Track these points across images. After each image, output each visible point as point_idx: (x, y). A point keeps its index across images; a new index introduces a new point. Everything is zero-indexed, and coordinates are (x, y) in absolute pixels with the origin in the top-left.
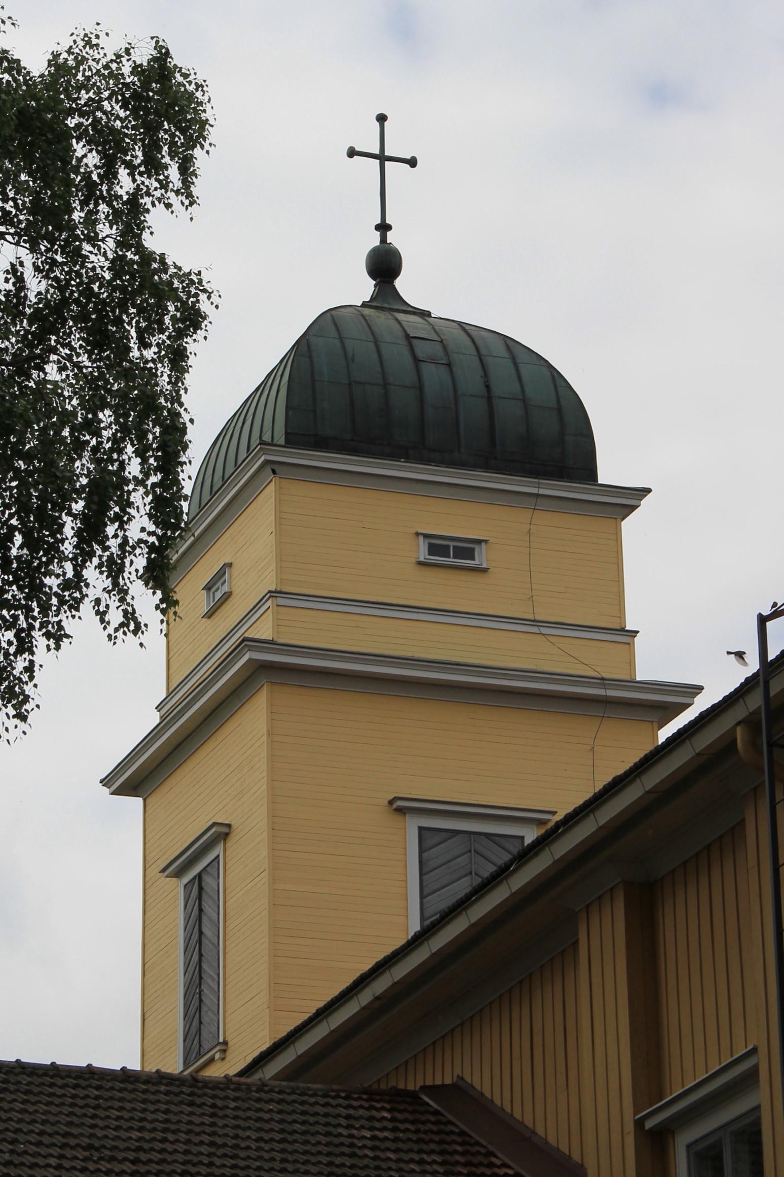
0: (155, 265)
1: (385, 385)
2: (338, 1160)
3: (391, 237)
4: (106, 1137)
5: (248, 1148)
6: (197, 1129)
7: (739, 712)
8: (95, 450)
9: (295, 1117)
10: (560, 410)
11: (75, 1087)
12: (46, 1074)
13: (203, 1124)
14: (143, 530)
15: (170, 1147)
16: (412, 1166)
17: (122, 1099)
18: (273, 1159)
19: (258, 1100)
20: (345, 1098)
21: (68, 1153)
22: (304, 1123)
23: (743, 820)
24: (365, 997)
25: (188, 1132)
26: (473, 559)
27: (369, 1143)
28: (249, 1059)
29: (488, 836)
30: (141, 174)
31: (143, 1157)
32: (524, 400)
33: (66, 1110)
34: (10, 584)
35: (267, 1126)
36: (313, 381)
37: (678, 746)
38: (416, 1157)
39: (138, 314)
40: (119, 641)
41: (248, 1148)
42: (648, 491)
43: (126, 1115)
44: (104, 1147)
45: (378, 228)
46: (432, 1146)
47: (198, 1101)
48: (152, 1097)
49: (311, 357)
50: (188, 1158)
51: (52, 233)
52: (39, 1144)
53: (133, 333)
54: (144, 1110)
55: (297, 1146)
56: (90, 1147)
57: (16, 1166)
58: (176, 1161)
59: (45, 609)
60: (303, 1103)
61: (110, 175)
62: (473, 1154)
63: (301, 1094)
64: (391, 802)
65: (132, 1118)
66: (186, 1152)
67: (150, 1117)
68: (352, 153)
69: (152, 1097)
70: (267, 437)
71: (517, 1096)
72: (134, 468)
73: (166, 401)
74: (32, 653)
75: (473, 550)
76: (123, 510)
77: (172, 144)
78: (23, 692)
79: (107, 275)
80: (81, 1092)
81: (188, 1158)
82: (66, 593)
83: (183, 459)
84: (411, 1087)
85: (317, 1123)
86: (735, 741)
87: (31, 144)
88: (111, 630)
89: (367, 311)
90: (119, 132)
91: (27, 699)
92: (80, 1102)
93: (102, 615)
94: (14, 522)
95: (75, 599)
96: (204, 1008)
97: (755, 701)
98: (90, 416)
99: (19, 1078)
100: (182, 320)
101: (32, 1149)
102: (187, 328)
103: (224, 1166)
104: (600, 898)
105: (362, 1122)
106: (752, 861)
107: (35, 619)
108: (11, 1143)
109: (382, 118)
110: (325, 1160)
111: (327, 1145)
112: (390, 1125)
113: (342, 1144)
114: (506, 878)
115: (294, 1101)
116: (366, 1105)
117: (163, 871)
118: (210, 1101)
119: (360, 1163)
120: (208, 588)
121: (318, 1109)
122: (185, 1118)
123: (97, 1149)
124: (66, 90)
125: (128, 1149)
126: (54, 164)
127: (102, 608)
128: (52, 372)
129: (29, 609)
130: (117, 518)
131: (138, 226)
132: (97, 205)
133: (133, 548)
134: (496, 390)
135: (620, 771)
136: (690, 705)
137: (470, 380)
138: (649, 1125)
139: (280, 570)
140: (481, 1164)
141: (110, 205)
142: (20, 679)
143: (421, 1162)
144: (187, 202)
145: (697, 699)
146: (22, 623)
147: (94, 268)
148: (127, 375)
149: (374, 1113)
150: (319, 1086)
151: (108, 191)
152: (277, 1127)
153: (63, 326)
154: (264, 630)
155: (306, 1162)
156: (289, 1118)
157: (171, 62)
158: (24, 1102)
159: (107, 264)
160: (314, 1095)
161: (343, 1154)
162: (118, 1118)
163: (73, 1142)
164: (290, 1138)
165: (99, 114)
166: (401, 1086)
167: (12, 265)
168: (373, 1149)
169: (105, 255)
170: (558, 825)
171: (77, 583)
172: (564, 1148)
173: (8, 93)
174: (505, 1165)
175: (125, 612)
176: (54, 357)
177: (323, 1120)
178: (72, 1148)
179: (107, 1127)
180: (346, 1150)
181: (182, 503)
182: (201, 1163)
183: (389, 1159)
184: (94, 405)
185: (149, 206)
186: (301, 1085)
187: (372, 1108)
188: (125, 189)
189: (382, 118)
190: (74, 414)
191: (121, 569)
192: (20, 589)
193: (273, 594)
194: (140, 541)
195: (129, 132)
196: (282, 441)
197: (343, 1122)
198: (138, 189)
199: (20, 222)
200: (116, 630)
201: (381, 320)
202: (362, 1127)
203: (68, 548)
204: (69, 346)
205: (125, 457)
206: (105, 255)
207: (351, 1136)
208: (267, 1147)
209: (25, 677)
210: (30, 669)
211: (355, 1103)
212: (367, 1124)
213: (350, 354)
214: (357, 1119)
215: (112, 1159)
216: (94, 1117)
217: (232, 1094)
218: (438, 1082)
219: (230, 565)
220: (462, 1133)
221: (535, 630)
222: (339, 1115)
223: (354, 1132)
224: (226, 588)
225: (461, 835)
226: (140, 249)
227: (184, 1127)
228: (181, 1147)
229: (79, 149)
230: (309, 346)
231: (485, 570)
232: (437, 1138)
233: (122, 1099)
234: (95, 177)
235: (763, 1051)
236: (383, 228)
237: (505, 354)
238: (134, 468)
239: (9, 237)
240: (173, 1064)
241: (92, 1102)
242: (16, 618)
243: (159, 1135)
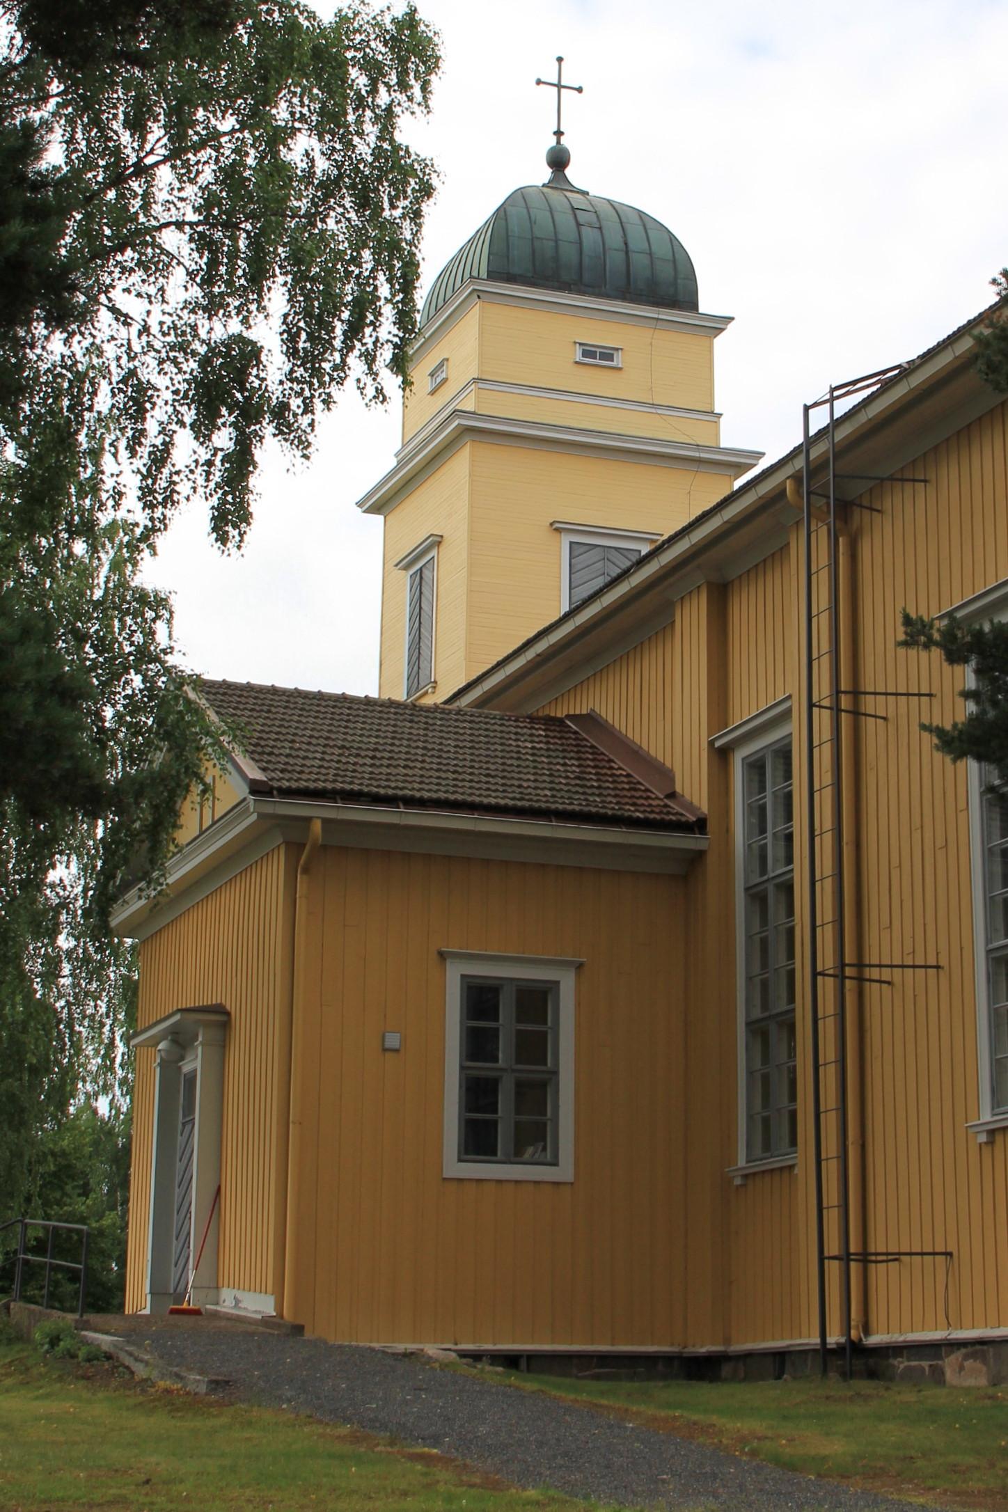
0: (402, 153)
1: (556, 241)
2: (509, 762)
3: (563, 140)
4: (354, 741)
5: (449, 751)
6: (415, 738)
7: (789, 470)
8: (358, 277)
9: (481, 732)
10: (674, 261)
11: (334, 707)
12: (314, 698)
13: (419, 735)
14: (390, 333)
15: (396, 749)
16: (558, 767)
17: (365, 716)
18: (465, 760)
19: (456, 720)
20: (515, 721)
21: (329, 750)
22: (486, 736)
23: (789, 543)
24: (530, 654)
25: (408, 740)
26: (612, 361)
27: (530, 751)
28: (451, 694)
29: (616, 549)
30: (395, 91)
31: (378, 755)
32: (650, 254)
33: (328, 722)
34: (299, 367)
35: (462, 738)
36: (508, 236)
37: (745, 493)
38: (561, 761)
39: (389, 186)
40: (372, 408)
41: (449, 751)
42: (733, 319)
43: (368, 727)
44: (352, 747)
45: (555, 133)
46: (572, 754)
47: (416, 719)
48: (386, 716)
49: (506, 220)
50: (408, 756)
51: (333, 129)
52: (309, 743)
53: (386, 199)
54: (380, 724)
55: (481, 752)
56: (343, 747)
57: (293, 757)
58: (400, 759)
59: (322, 384)
60: (486, 723)
61: (374, 91)
62: (599, 760)
63: (486, 717)
64: (551, 524)
65: (371, 729)
66: (407, 753)
67: (383, 729)
68: (539, 82)
69: (386, 716)
70: (475, 274)
71: (630, 722)
72: (384, 291)
73: (407, 244)
74: (313, 414)
75: (613, 355)
76: (376, 318)
77: (417, 71)
78: (307, 441)
79: (370, 159)
80: (338, 711)
81: (408, 756)
82: (335, 374)
83: (417, 284)
84: (559, 715)
85: (495, 737)
86: (785, 490)
87: (321, 69)
88: (367, 400)
89: (546, 190)
90: (381, 62)
91: (309, 444)
92: (337, 717)
93: (361, 389)
94: (302, 324)
95: (340, 377)
96: (422, 659)
97: (800, 463)
98: (355, 254)
99: (297, 700)
100: (419, 191)
101: (305, 747)
102: (423, 197)
103: (432, 763)
104: (691, 592)
105: (526, 737)
106: (794, 571)
107: (315, 390)
108: (290, 742)
109: (560, 60)
110: (500, 761)
111: (502, 751)
112: (544, 740)
113: (512, 751)
114: (628, 577)
115: (480, 722)
116: (529, 726)
117: (397, 565)
118: (424, 720)
119: (524, 764)
120: (432, 375)
121: (496, 727)
122: (407, 730)
123: (348, 749)
124: (346, 33)
125: (368, 749)
126: (336, 83)
127: (362, 385)
128: (331, 223)
129: (311, 384)
130: (372, 323)
131: (392, 126)
132: (364, 111)
133: (382, 344)
134: (632, 246)
135: (707, 508)
136: (755, 465)
137: (614, 239)
138: (717, 744)
139: (481, 364)
140: (604, 767)
141: (373, 111)
142: (305, 431)
143: (565, 765)
144: (425, 111)
145: (761, 461)
146: (307, 393)
147: (360, 154)
148: (382, 227)
149: (534, 731)
150: (498, 712)
151: (372, 102)
152: (469, 738)
153: (339, 192)
154: (469, 405)
155: (487, 762)
156: (476, 733)
157: (417, 17)
158: (300, 716)
159: (370, 151)
160: (494, 718)
161: (512, 758)
162: (362, 729)
163: (331, 743)
164: (477, 746)
165: (368, 50)
166: (553, 714)
167: (306, 151)
168: (533, 755)
169: (368, 145)
170: (664, 543)
171: (342, 366)
172: (660, 759)
173: (307, 34)
174: (620, 768)
175: (377, 388)
176: (332, 214)
177: (499, 735)
178: (331, 747)
179: (355, 734)
180: (515, 755)
181: (416, 314)
182: (417, 760)
183: (543, 762)
184: (358, 246)
185: (400, 113)
186: (486, 711)
187: (532, 728)
188: (384, 101)
189: (560, 60)
190: (344, 252)
191: (374, 360)
192: (306, 370)
193: (476, 380)
194: (388, 341)
195: (388, 63)
196: (485, 277)
197: (513, 737)
198: (393, 101)
199: (312, 121)
200: (370, 400)
201: (555, 196)
202: (526, 741)
203: (337, 343)
204: (343, 206)
205: (377, 282)
206: (368, 145)
207: (518, 746)
208: (461, 751)
209: (308, 430)
210: (312, 425)
211: (521, 725)
212: (529, 739)
213: (533, 218)
214: (522, 735)
215: (358, 755)
216: (346, 727)
217: (439, 716)
218: (578, 712)
219: (447, 360)
220: (592, 747)
221: (653, 411)
222: (510, 732)
223: (520, 743)
224: (444, 375)
225: (598, 549)
226: (392, 141)
227: (406, 736)
228: (404, 749)
229: (354, 72)
230: (505, 212)
231: (620, 369)
232: (575, 749)
233: (365, 716)
234: (363, 93)
235: (795, 698)
236: (559, 133)
237: (639, 222)
238: (384, 291)
239: (304, 131)
240: (400, 695)
241: (345, 718)
242: (302, 389)
243: (389, 741)
